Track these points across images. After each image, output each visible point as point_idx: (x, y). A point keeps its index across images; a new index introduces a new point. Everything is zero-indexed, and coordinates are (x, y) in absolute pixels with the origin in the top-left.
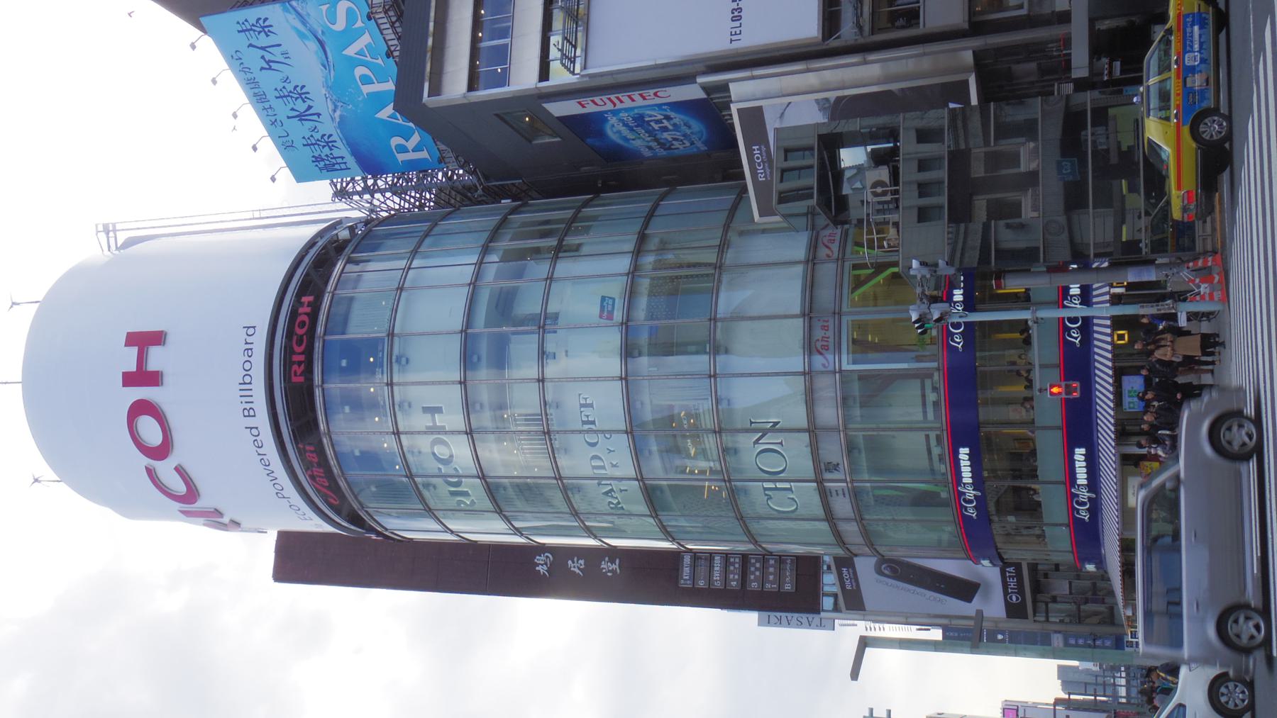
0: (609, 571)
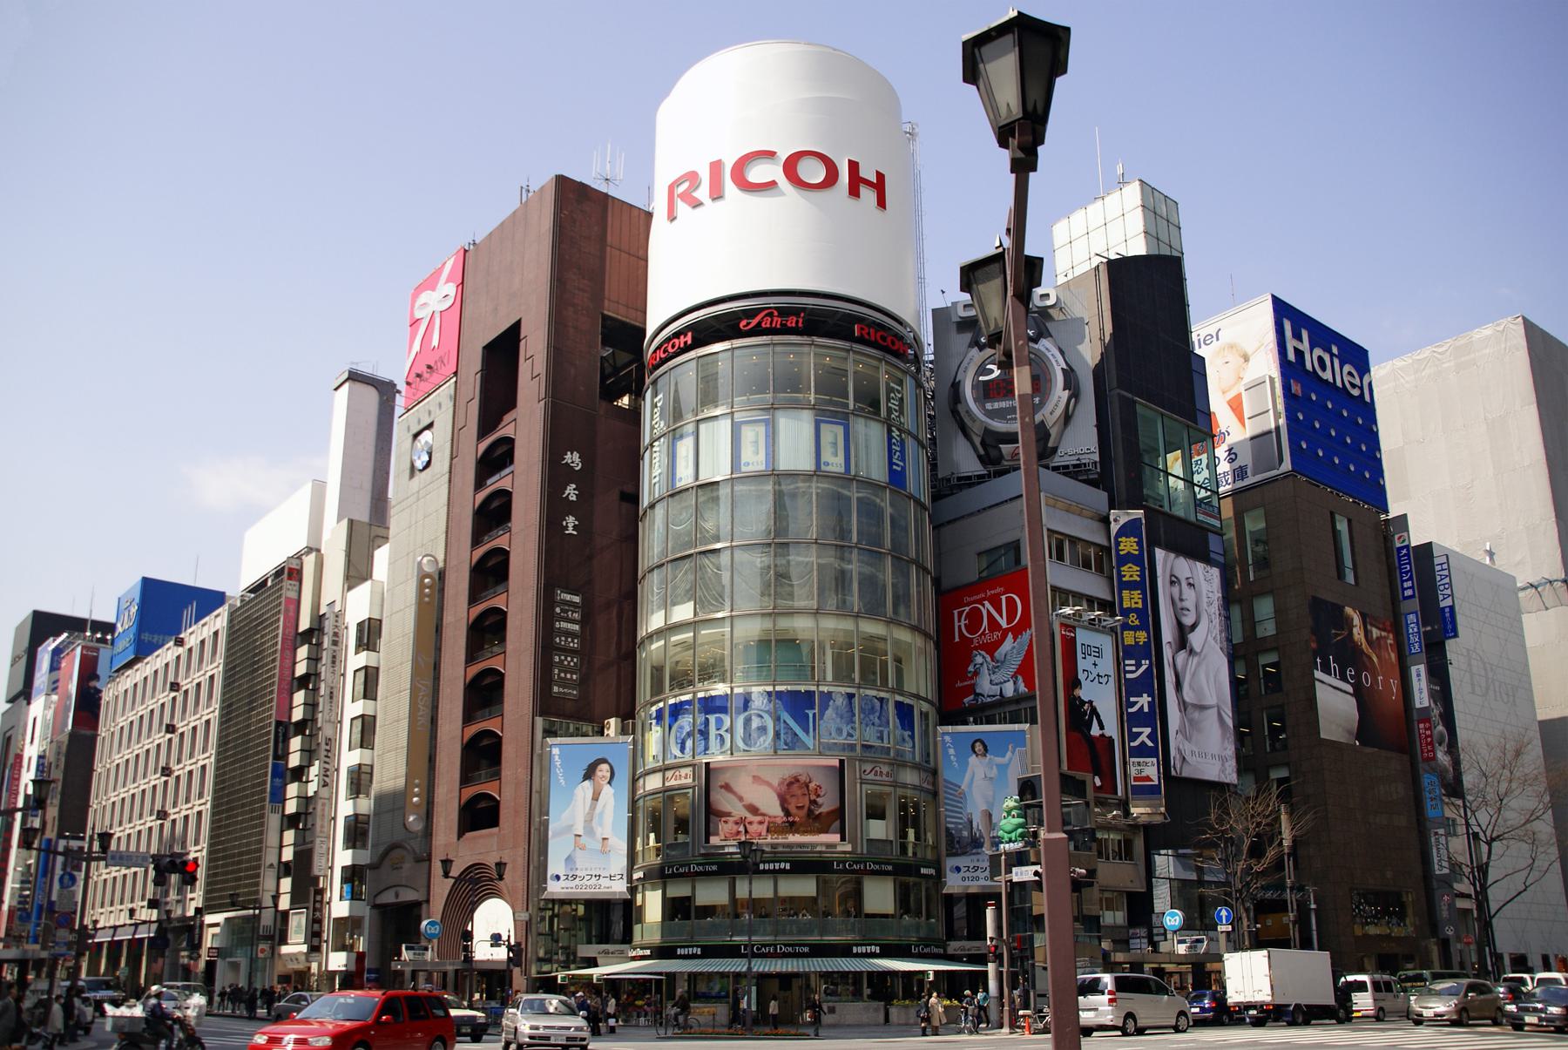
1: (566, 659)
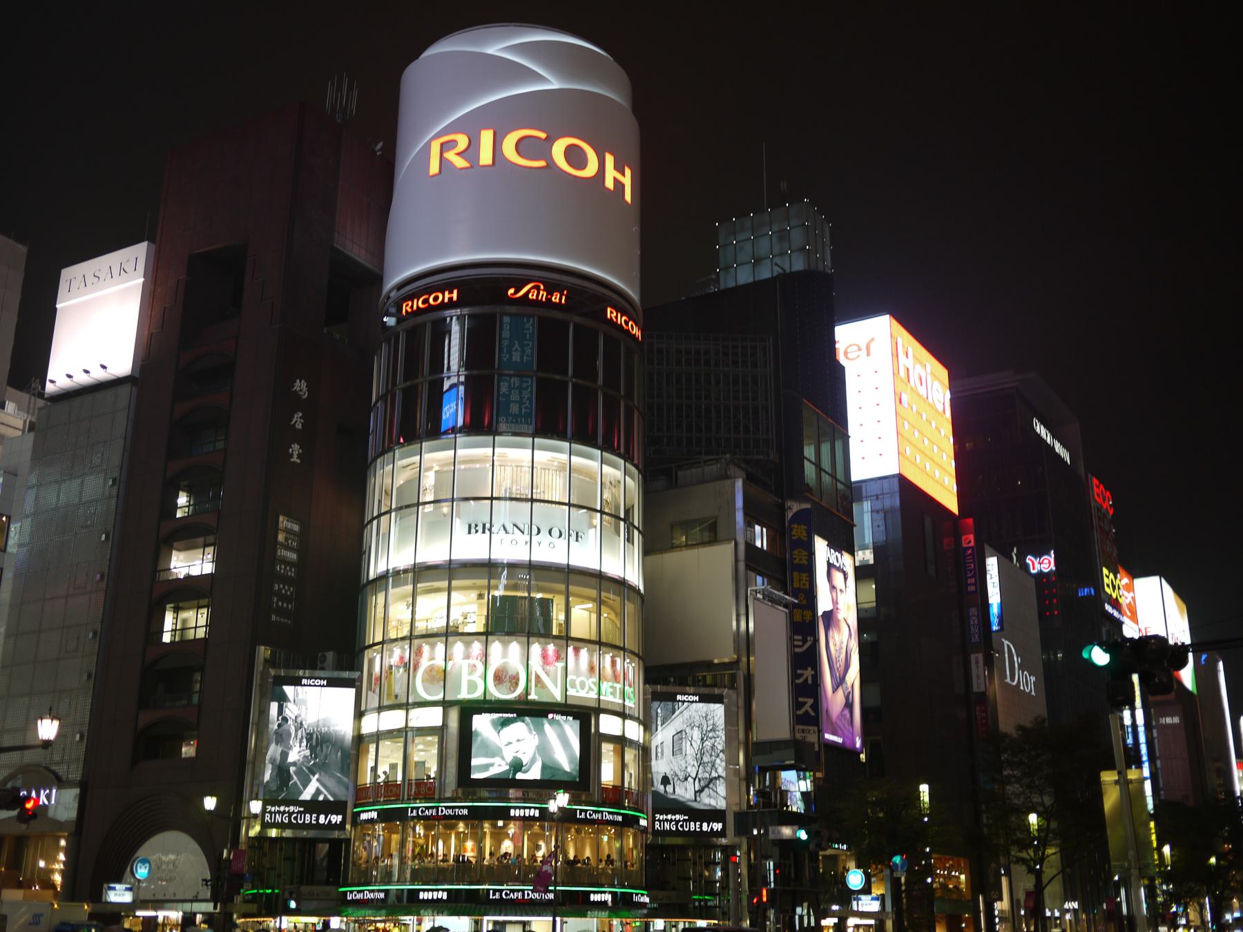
1: (284, 588)
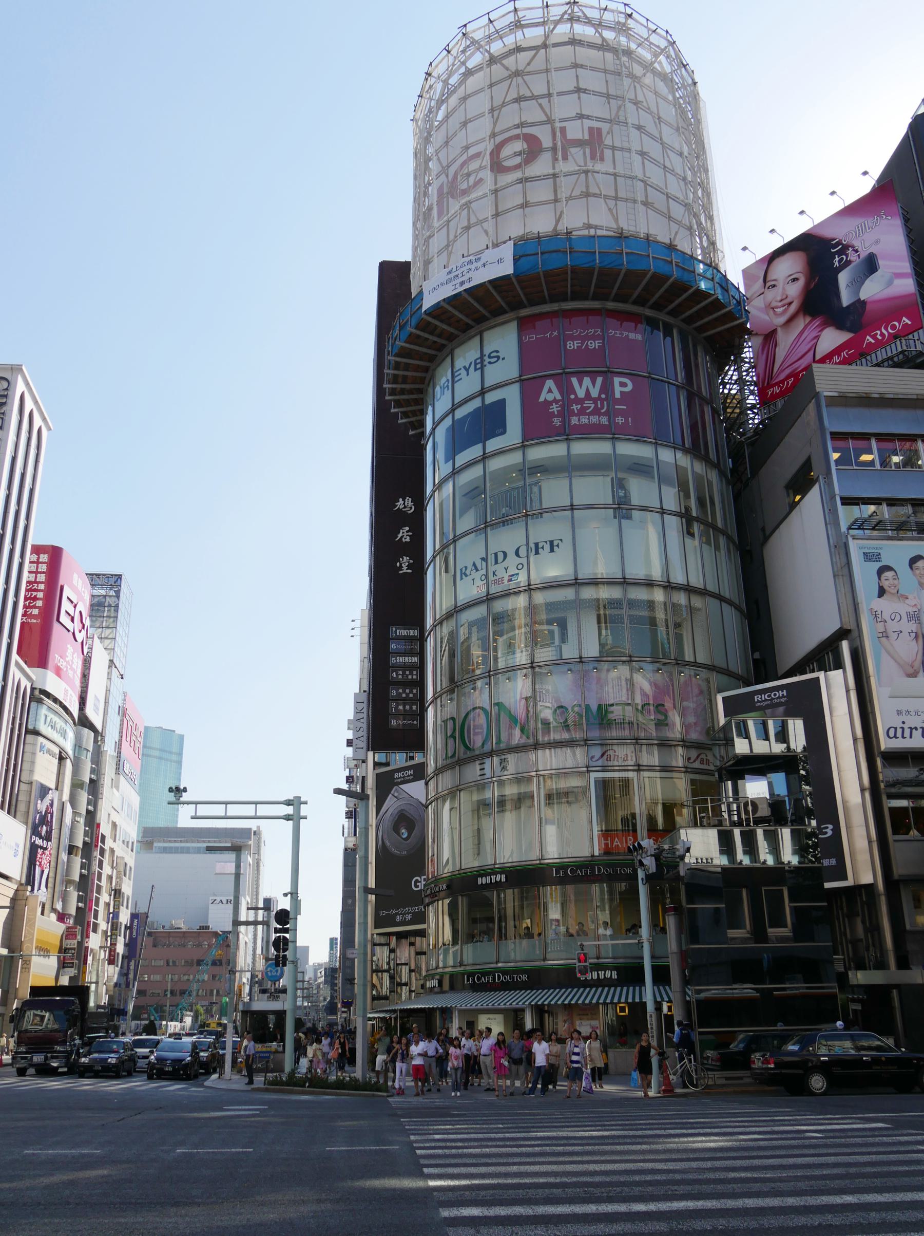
0: (401, 564)
1: (404, 692)
